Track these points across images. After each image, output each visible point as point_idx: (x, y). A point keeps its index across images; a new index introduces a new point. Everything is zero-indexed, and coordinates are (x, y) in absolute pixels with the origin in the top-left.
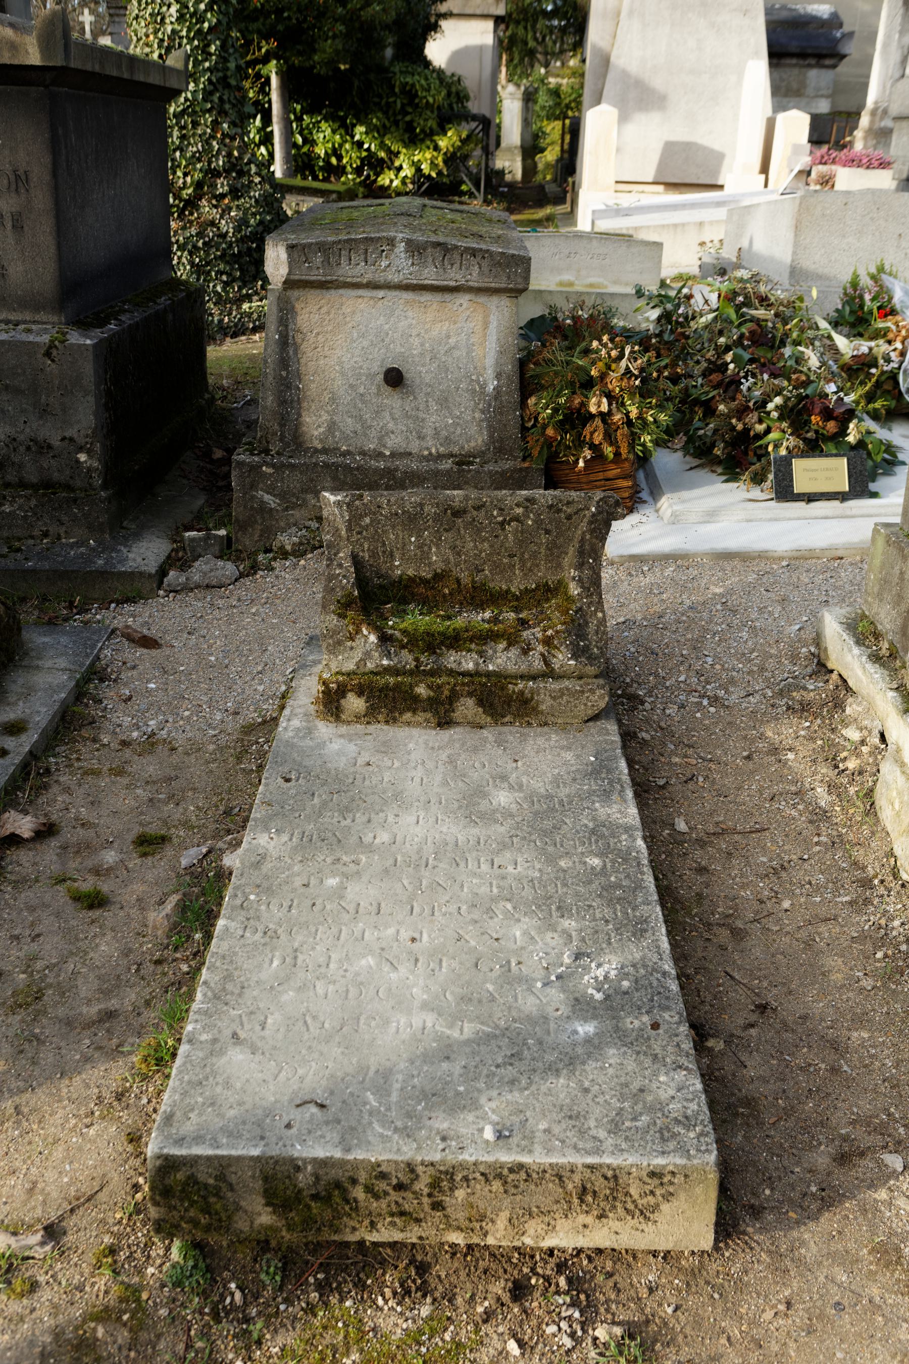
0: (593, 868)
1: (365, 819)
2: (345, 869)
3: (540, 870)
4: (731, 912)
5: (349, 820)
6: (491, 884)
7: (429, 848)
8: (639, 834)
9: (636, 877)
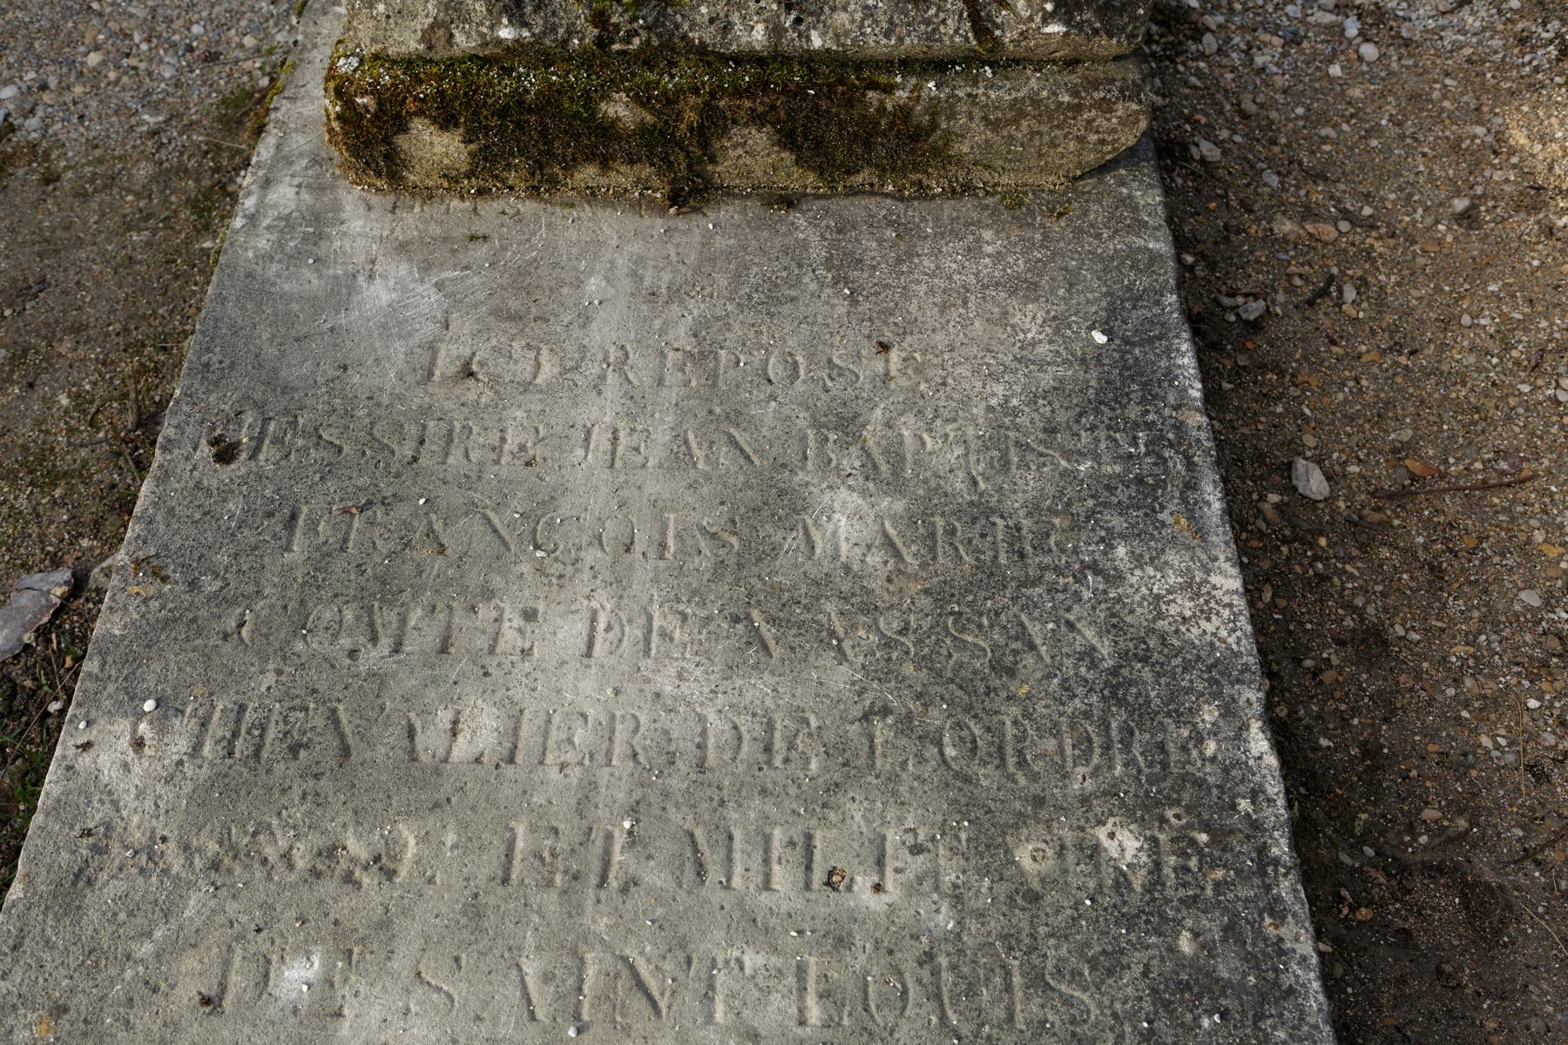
0: (1122, 882)
1: (431, 637)
2: (344, 904)
3: (957, 899)
4: (1462, 823)
5: (385, 643)
6: (801, 970)
7: (616, 784)
8: (1251, 696)
9: (1259, 933)
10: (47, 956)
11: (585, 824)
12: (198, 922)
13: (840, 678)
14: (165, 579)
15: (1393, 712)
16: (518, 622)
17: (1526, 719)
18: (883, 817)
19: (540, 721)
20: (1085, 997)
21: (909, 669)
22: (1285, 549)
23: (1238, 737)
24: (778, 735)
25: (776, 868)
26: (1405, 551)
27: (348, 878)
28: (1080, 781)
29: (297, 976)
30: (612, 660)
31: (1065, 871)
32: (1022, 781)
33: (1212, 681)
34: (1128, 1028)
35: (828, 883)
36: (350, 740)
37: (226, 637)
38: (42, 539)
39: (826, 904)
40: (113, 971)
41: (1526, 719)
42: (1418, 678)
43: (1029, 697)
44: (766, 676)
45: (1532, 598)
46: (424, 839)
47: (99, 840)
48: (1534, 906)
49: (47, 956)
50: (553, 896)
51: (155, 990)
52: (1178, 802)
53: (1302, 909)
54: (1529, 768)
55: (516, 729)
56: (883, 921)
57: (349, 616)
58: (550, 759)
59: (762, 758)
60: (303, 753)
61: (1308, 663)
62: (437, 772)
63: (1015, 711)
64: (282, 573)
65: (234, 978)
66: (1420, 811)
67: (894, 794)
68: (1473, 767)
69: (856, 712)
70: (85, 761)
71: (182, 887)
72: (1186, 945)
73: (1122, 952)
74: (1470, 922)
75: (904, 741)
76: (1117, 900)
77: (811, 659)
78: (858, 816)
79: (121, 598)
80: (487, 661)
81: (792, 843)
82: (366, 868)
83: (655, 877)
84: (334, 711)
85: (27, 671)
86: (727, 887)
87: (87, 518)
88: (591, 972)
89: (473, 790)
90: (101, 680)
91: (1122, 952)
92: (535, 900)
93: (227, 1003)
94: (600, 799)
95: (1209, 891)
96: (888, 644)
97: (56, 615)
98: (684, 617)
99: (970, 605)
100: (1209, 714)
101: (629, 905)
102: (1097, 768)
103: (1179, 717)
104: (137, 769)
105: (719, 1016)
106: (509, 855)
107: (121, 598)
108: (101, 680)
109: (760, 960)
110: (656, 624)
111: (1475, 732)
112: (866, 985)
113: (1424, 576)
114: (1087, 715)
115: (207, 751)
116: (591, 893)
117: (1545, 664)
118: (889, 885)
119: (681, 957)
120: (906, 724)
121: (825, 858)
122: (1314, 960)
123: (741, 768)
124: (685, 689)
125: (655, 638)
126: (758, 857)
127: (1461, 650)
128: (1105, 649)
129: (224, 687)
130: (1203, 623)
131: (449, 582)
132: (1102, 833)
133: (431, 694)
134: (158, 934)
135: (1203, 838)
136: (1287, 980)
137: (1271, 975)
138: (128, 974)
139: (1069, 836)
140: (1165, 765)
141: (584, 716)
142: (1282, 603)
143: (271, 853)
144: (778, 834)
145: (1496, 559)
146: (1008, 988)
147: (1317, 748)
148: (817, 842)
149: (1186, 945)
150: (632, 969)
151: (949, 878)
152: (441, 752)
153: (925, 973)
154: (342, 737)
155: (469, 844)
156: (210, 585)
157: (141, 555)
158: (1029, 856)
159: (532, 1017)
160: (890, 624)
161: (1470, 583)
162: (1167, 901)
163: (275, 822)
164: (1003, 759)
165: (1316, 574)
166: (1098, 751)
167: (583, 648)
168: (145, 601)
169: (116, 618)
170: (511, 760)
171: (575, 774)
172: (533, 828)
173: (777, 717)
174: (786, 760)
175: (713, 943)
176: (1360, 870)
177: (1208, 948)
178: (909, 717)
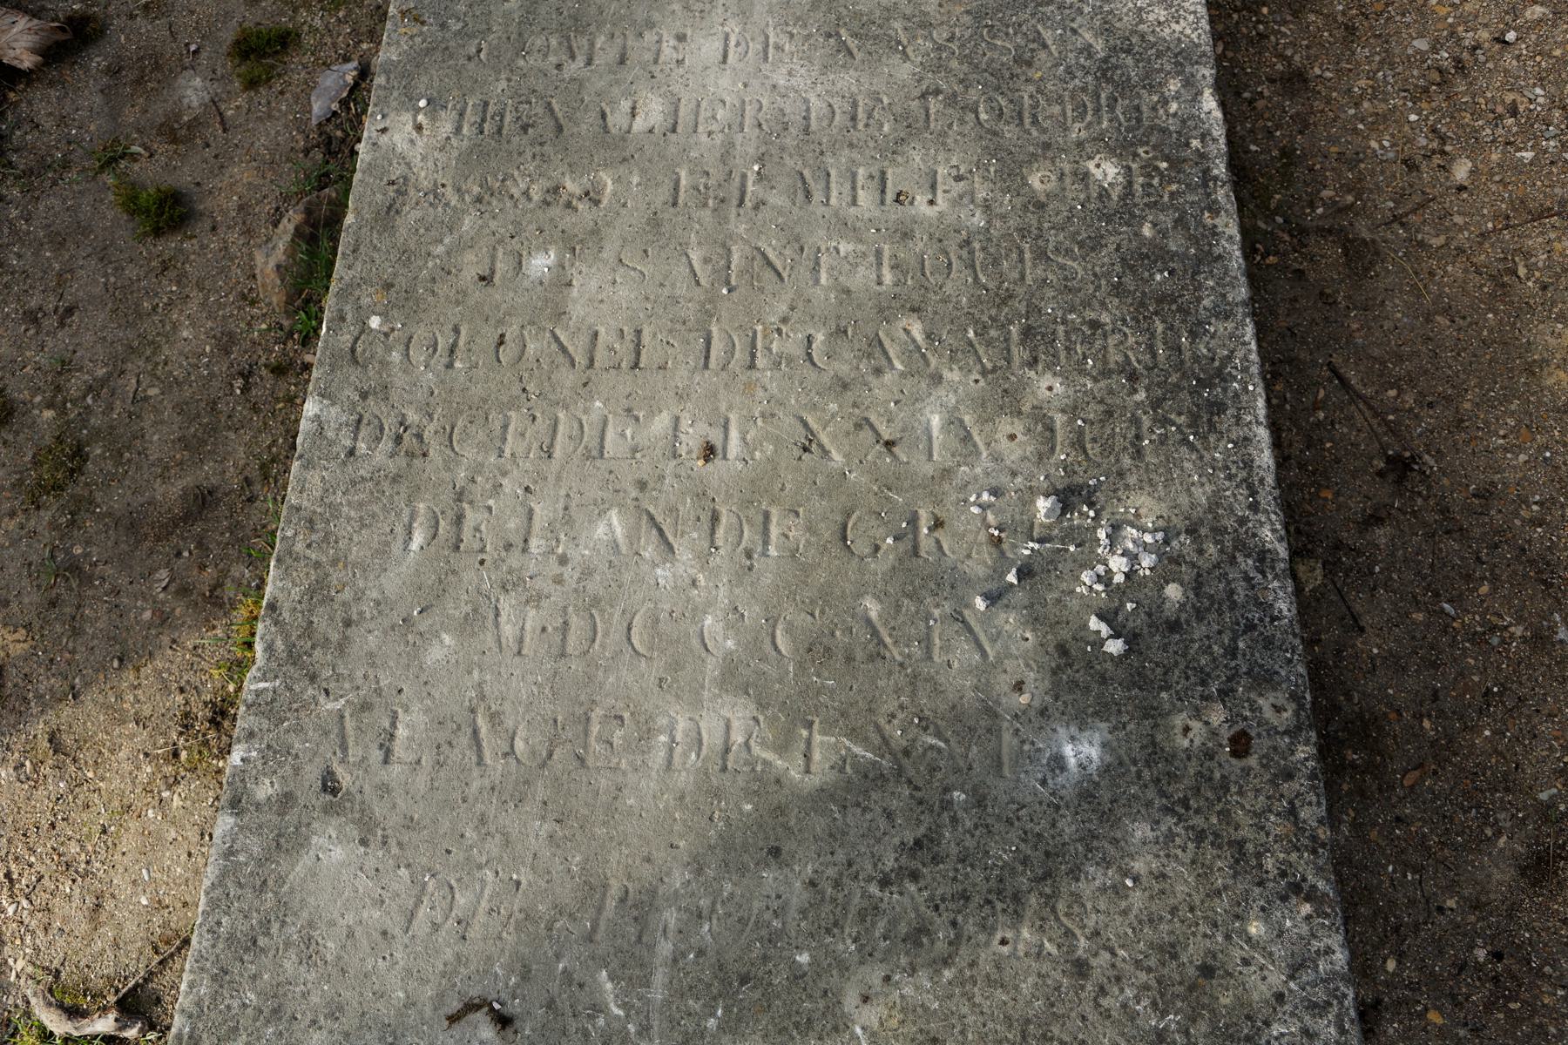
0: (1104, 194)
1: (613, 54)
2: (568, 221)
3: (987, 207)
4: (1350, 198)
5: (581, 60)
6: (879, 253)
7: (747, 143)
8: (1207, 72)
9: (1200, 223)
10: (376, 255)
11: (727, 169)
12: (472, 233)
13: (905, 71)
14: (423, 23)
15: (1307, 126)
16: (673, 42)
17: (1407, 128)
18: (935, 159)
19: (693, 105)
20: (1075, 265)
21: (954, 64)
22: (1235, 16)
23: (1194, 100)
24: (860, 110)
25: (860, 192)
26: (1327, 16)
27: (569, 205)
28: (1077, 132)
29: (540, 263)
30: (741, 65)
31: (1064, 189)
32: (1035, 133)
33: (1177, 64)
34: (1103, 282)
35: (897, 201)
36: (561, 121)
37: (469, 59)
38: (334, 45)
39: (895, 213)
40: (420, 263)
41: (1407, 128)
42: (1328, 102)
43: (1041, 79)
44: (852, 72)
45: (1422, 45)
46: (618, 180)
47: (400, 187)
48: (1396, 252)
49: (376, 255)
50: (708, 212)
51: (449, 273)
52: (1147, 143)
53: (1232, 207)
54: (1404, 162)
55: (676, 111)
56: (935, 222)
57: (554, 42)
58: (701, 129)
59: (849, 124)
60: (530, 131)
61: (1246, 95)
62: (623, 139)
63: (1031, 88)
64: (504, 16)
65: (499, 265)
66: (1319, 191)
67: (943, 144)
68: (1361, 161)
69: (917, 93)
70: (384, 140)
71: (458, 214)
72: (1147, 231)
73: (1102, 237)
74: (1347, 264)
75: (951, 111)
76: (1101, 205)
77: (884, 59)
78: (917, 159)
79: (395, 36)
80: (653, 68)
81: (871, 177)
82: (580, 199)
83: (776, 199)
84: (549, 104)
85: (337, 127)
86: (827, 204)
87: (363, 29)
88: (736, 258)
89: (649, 149)
90: (388, 89)
91: (1102, 237)
92: (696, 215)
93: (497, 279)
94: (737, 153)
95: (1166, 198)
96: (939, 48)
97: (351, 91)
98: (792, 36)
99: (1000, 20)
100: (1174, 86)
101: (760, 216)
102: (1090, 123)
103: (1151, 88)
104: (419, 143)
105: (823, 281)
106: (676, 189)
107: (395, 36)
108: (388, 89)
109: (851, 247)
110: (771, 41)
111: (1367, 138)
112: (923, 260)
113: (1339, 33)
114: (1084, 90)
115: (465, 130)
116: (734, 211)
117: (1426, 90)
118: (939, 200)
119: (797, 246)
120: (952, 100)
121: (894, 185)
122: (1238, 238)
123: (835, 131)
124: (793, 81)
125: (771, 50)
126: (848, 186)
127: (1363, 83)
128: (1099, 46)
129: (472, 91)
130: (1174, 26)
131: (622, 18)
132: (1091, 165)
133: (616, 90)
134: (447, 241)
135: (1164, 165)
136: (1217, 251)
137: (1206, 248)
138: (430, 264)
139: (1067, 168)
140: (1139, 120)
141: (723, 102)
142: (1230, 54)
143: (515, 191)
144: (861, 171)
145: (1398, 18)
146: (1022, 260)
147: (1248, 151)
148: (889, 176)
149: (1147, 231)
150: (763, 254)
151: (981, 195)
152: (625, 127)
153: (964, 253)
154: (556, 120)
155: (648, 182)
156: (455, 26)
157: (404, 8)
158: (1038, 181)
159: (698, 283)
160: (940, 35)
161: (1376, 36)
162: (1136, 205)
163: (516, 173)
164: (1021, 119)
165: (1258, 34)
166: (1090, 112)
167: (720, 58)
168: (412, 37)
169: (393, 49)
170: (674, 131)
171: (718, 138)
172: (691, 172)
173: (860, 98)
174: (867, 125)
175: (818, 237)
176: (1272, 233)
177: (1164, 234)
178: (955, 95)
